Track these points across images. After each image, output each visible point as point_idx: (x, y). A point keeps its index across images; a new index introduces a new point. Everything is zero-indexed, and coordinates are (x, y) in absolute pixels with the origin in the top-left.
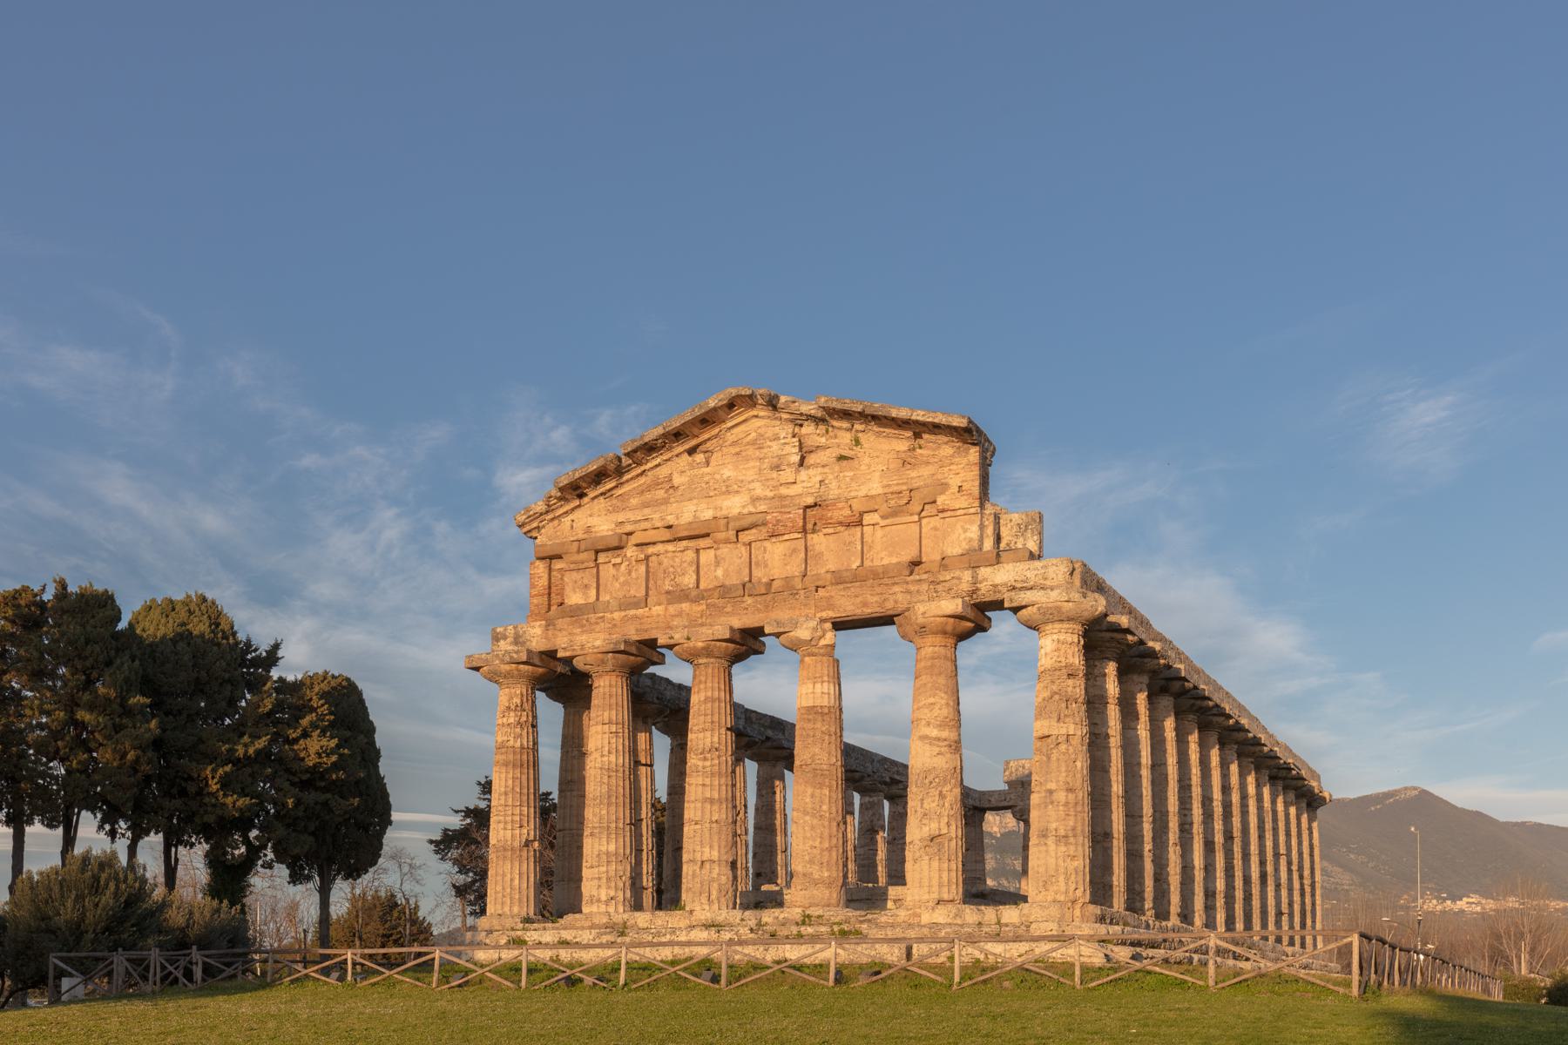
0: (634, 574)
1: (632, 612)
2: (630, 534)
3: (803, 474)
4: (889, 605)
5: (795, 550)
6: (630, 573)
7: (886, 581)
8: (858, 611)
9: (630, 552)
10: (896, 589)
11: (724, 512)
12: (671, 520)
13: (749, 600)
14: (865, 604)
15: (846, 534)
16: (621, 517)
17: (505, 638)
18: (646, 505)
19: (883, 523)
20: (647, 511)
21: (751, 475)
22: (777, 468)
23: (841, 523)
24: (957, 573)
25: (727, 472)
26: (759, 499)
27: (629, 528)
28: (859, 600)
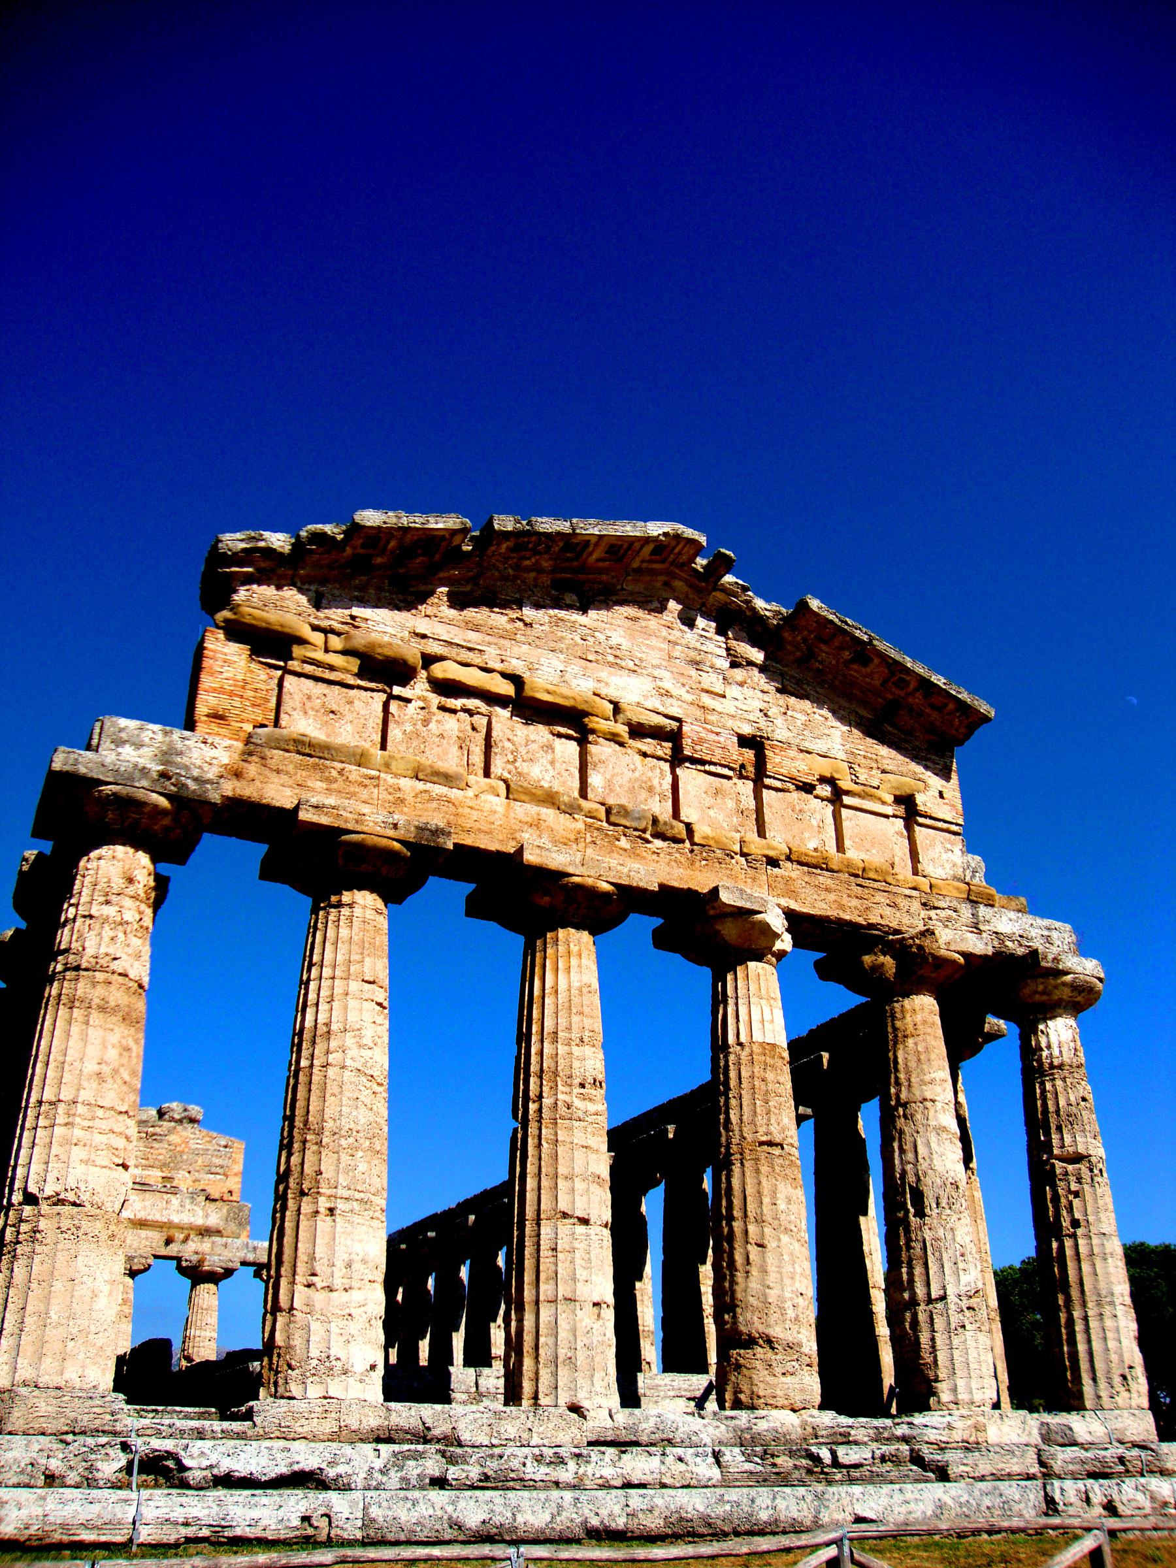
0: (433, 726)
1: (438, 790)
2: (429, 660)
3: (733, 691)
4: (874, 919)
5: (717, 792)
6: (426, 722)
7: (866, 883)
8: (829, 913)
9: (419, 688)
10: (880, 897)
11: (614, 694)
12: (516, 666)
13: (658, 843)
14: (842, 907)
15: (796, 796)
16: (423, 626)
17: (139, 746)
18: (476, 628)
19: (847, 800)
20: (473, 636)
21: (654, 658)
22: (696, 664)
23: (792, 778)
24: (955, 904)
25: (618, 637)
26: (668, 694)
27: (434, 648)
28: (832, 897)
